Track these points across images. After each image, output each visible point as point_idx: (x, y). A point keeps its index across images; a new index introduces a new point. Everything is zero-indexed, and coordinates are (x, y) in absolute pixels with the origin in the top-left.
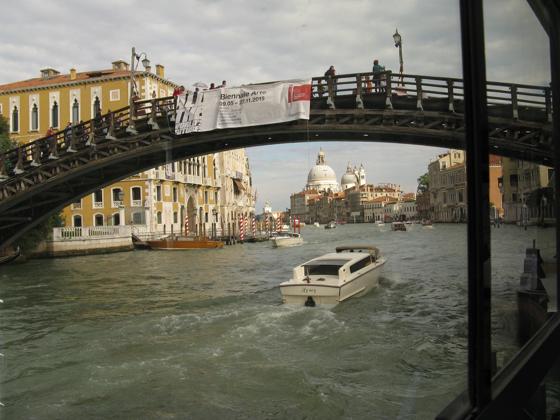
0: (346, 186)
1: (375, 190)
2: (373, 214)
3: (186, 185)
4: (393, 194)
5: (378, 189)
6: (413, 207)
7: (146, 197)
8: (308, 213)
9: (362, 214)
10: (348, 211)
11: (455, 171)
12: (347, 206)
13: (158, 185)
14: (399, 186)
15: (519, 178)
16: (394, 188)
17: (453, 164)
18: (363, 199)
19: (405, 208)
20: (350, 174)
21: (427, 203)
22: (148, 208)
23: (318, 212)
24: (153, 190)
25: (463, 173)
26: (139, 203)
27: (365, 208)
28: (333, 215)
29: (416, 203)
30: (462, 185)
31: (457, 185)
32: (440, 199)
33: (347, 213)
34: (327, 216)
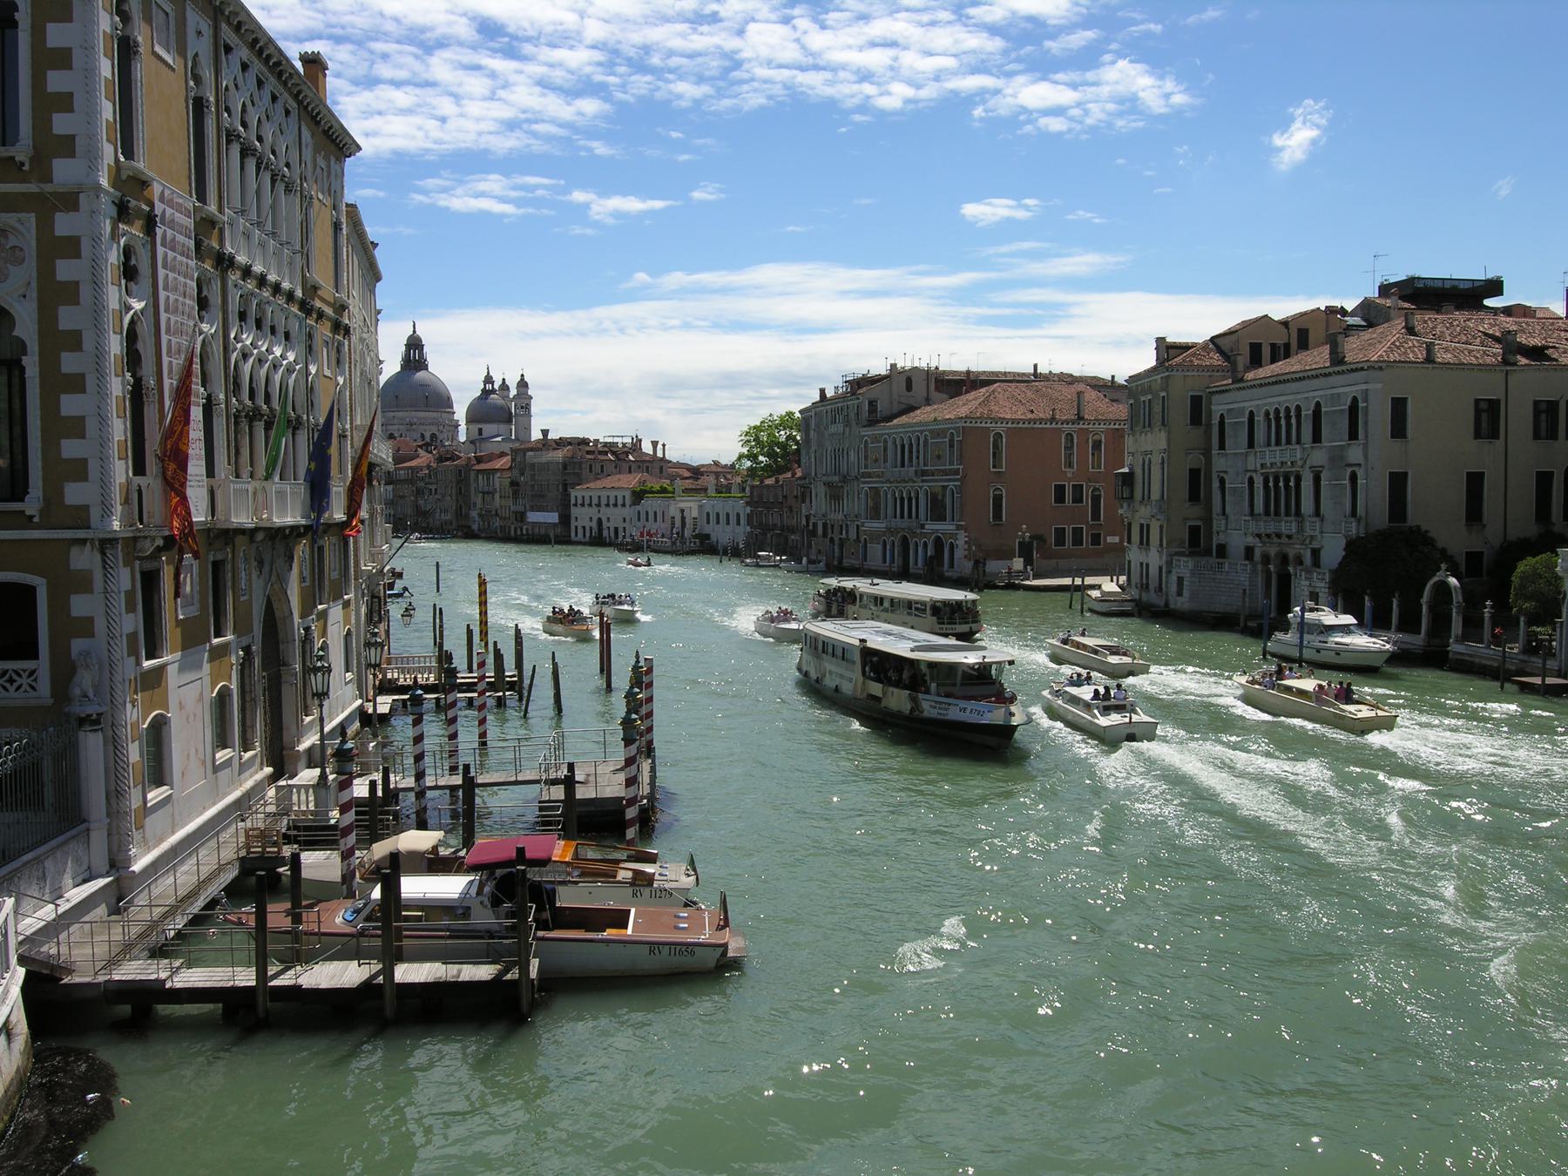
0: (480, 431)
2: (600, 521)
3: (260, 536)
4: (647, 468)
6: (738, 515)
7: (78, 645)
9: (565, 519)
10: (521, 509)
11: (921, 432)
12: (516, 494)
13: (149, 566)
14: (664, 445)
15: (1222, 481)
16: (647, 448)
17: (895, 409)
19: (708, 514)
21: (791, 508)
22: (93, 722)
23: (421, 502)
24: (120, 602)
25: (951, 441)
26: (24, 681)
27: (573, 502)
28: (467, 516)
30: (945, 472)
31: (924, 473)
32: (854, 504)
33: (516, 513)
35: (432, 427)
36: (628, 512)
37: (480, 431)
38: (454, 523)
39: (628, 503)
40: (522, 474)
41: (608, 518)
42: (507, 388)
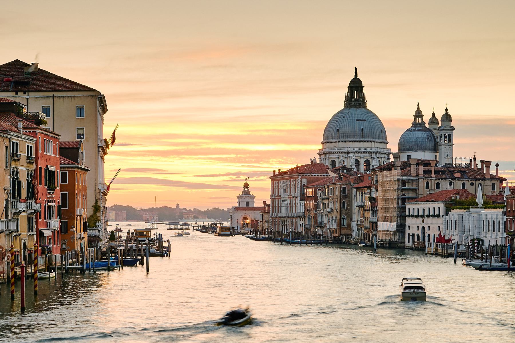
0: (409, 157)
1: (436, 172)
2: (423, 228)
5: (444, 172)
6: (499, 221)
8: (302, 216)
9: (401, 228)
10: (374, 220)
14: (497, 165)
18: (404, 193)
20: (419, 130)
27: (407, 213)
29: (505, 214)
33: (372, 223)
34: (335, 227)
35: (367, 155)
36: (440, 222)
37: (409, 157)
38: (338, 232)
39: (441, 214)
40: (377, 191)
41: (429, 227)
42: (437, 122)
